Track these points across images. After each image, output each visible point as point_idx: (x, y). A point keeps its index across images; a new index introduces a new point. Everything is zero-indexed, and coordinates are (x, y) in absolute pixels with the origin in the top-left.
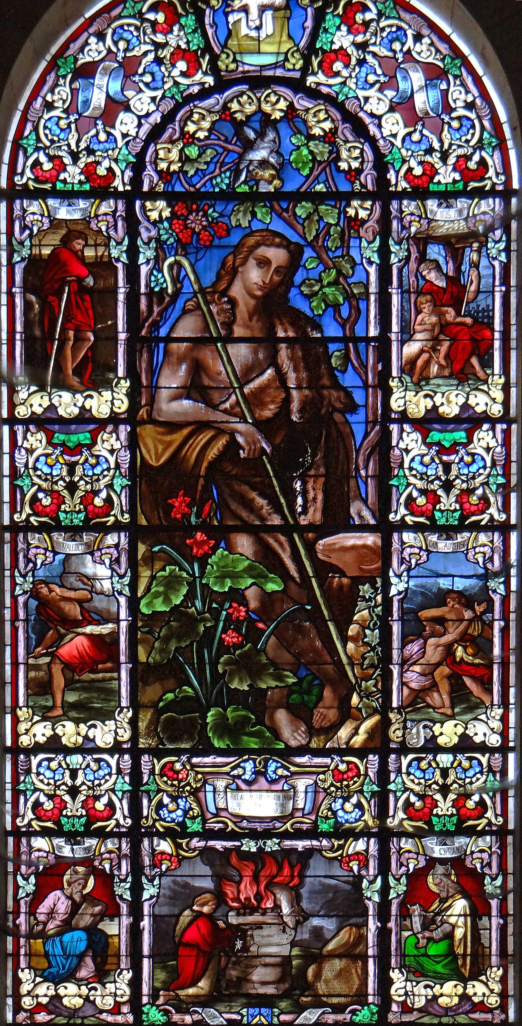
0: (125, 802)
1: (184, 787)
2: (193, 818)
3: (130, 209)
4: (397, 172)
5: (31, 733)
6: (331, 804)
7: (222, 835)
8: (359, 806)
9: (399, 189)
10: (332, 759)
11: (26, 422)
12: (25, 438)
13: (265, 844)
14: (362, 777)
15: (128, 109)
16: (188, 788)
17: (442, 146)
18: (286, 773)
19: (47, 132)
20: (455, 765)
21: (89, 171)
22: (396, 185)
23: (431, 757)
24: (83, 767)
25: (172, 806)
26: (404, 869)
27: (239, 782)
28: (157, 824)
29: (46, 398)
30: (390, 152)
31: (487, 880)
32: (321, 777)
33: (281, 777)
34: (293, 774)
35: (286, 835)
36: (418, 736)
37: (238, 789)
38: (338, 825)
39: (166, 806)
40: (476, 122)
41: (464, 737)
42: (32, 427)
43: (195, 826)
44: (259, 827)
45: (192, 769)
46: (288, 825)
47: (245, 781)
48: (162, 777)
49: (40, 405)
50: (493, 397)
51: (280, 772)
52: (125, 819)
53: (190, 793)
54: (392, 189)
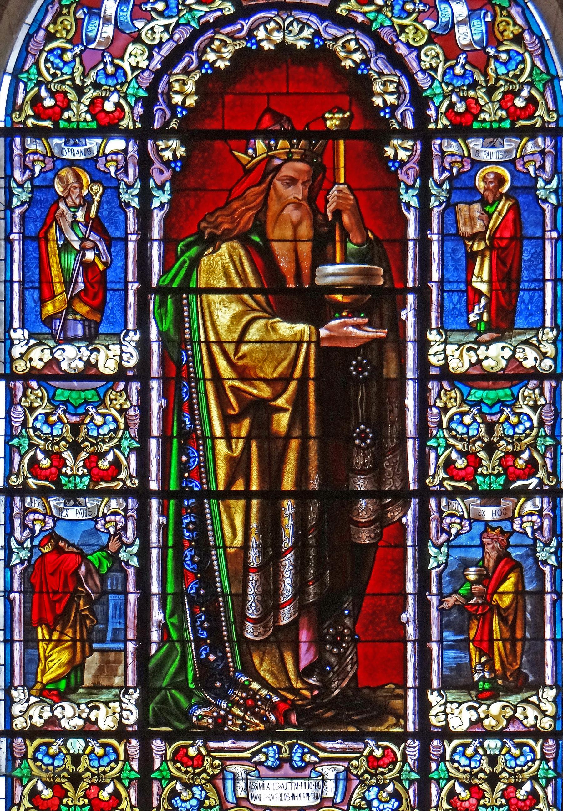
0: (132, 791)
1: (199, 774)
3: (142, 151)
4: (437, 109)
6: (364, 793)
8: (395, 795)
9: (440, 126)
10: (366, 745)
12: (25, 395)
14: (398, 765)
15: (138, 40)
16: (204, 775)
17: (487, 82)
18: (313, 759)
19: (49, 65)
20: (503, 752)
21: (95, 107)
22: (436, 122)
23: (476, 743)
24: (87, 752)
25: (186, 795)
29: (47, 352)
30: (430, 86)
32: (354, 762)
33: (308, 764)
34: (322, 760)
36: (461, 720)
40: (527, 55)
45: (209, 755)
47: (269, 768)
48: (175, 764)
49: (41, 359)
50: (543, 350)
51: (307, 758)
53: (208, 781)
54: (431, 126)
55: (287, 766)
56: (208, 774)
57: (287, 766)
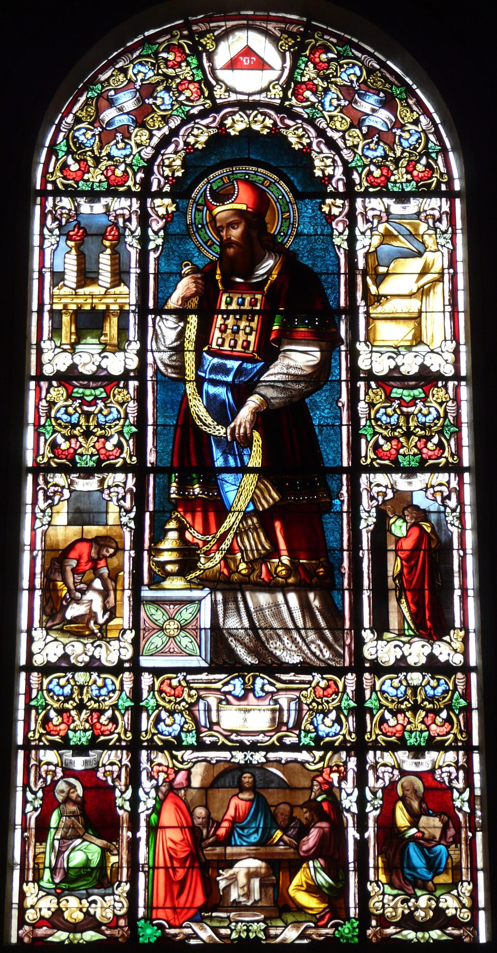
2: (189, 731)
5: (44, 653)
7: (214, 747)
10: (313, 677)
11: (49, 379)
12: (48, 392)
13: (252, 756)
16: (183, 704)
18: (272, 689)
25: (169, 721)
26: (381, 781)
27: (230, 698)
28: (155, 738)
31: (456, 794)
32: (304, 692)
33: (267, 693)
34: (279, 690)
35: (272, 748)
37: (229, 703)
38: (318, 739)
39: (164, 721)
41: (431, 657)
42: (54, 383)
43: (190, 739)
44: (247, 740)
46: (274, 739)
51: (268, 688)
52: (125, 734)
55: (251, 695)
56: (187, 703)
57: (251, 695)
